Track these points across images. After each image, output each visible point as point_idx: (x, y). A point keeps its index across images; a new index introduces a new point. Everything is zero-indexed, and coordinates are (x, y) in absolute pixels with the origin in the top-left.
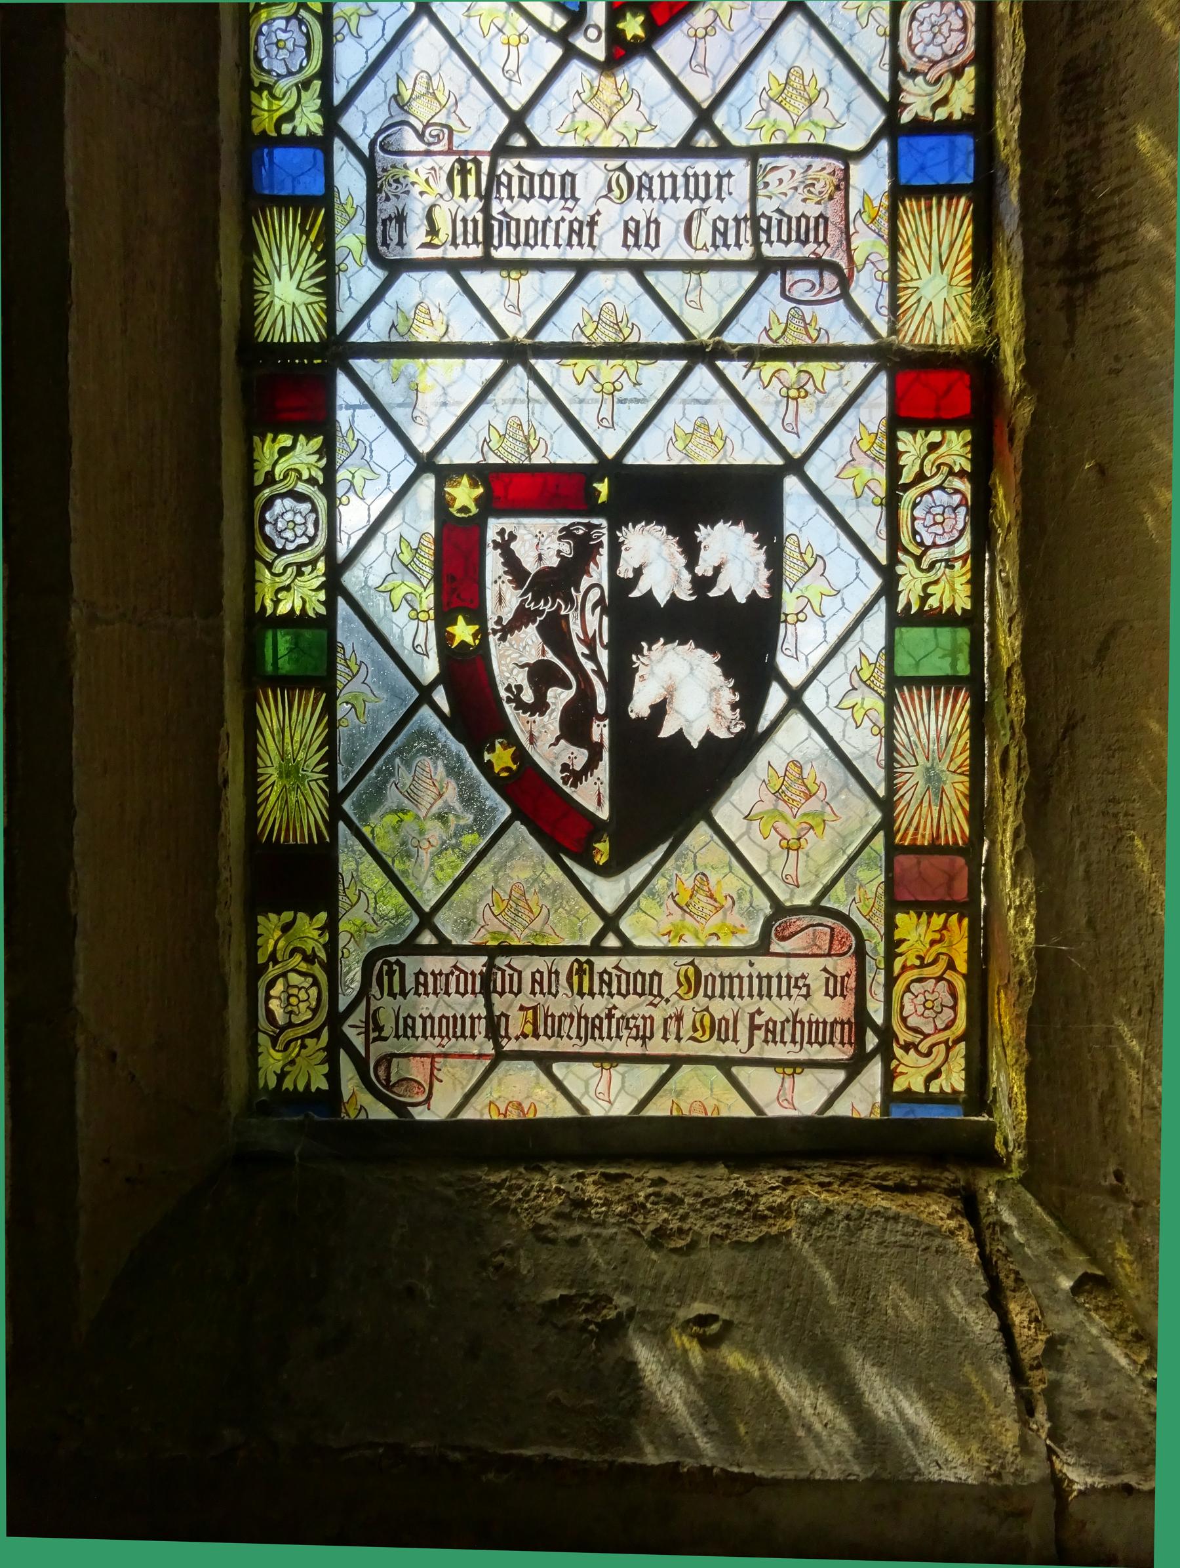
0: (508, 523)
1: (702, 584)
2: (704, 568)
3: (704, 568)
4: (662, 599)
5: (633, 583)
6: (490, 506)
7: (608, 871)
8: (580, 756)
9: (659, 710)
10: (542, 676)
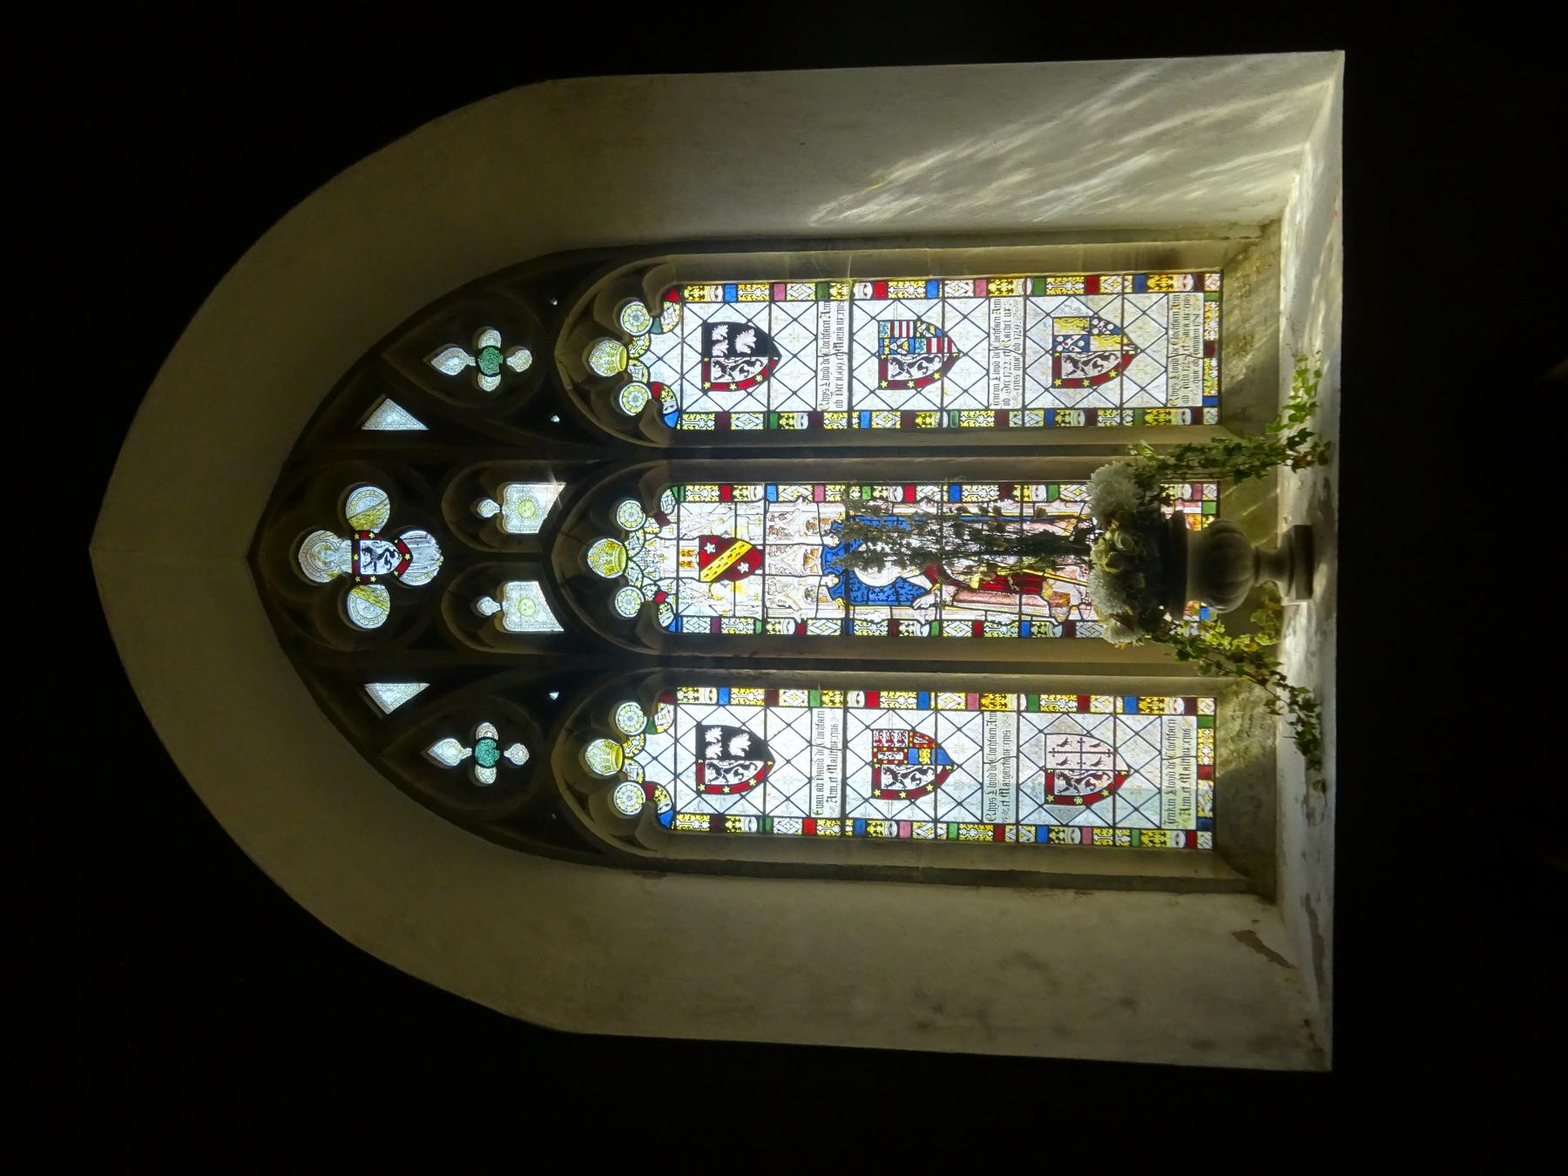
0: (706, 780)
1: (718, 741)
2: (715, 741)
3: (715, 741)
4: (721, 749)
5: (718, 755)
6: (704, 784)
7: (774, 762)
8: (752, 767)
9: (743, 750)
10: (736, 774)
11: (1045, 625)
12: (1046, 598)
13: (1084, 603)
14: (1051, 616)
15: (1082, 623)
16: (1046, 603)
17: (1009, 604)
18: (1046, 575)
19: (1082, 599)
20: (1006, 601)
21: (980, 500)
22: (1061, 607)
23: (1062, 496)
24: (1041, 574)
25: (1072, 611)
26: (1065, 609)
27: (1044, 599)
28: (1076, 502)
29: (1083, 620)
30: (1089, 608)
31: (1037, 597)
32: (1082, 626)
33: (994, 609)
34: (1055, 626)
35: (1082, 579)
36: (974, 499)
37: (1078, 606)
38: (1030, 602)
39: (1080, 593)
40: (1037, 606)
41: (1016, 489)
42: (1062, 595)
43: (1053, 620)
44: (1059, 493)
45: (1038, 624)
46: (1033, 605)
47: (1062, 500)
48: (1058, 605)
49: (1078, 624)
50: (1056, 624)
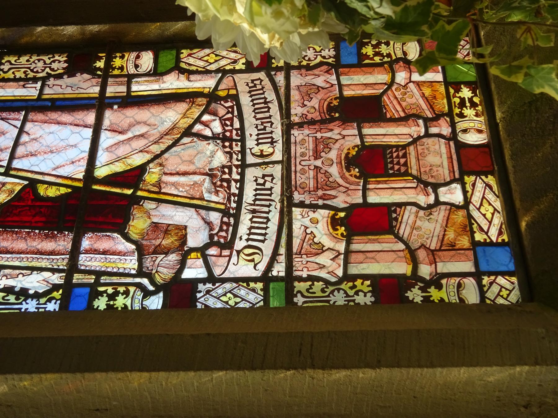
11: (127, 293)
12: (135, 237)
13: (218, 244)
14: (140, 273)
15: (209, 286)
16: (134, 247)
17: (52, 253)
18: (140, 193)
19: (211, 236)
20: (49, 245)
21: (31, 75)
22: (167, 254)
23: (183, 65)
24: (129, 192)
25: (189, 262)
26: (173, 258)
27: (128, 239)
28: (207, 72)
29: (211, 279)
30: (226, 252)
31: (115, 235)
32: (208, 292)
33: (17, 263)
34: (147, 294)
35: (214, 198)
36: (18, 75)
37: (202, 250)
38: (104, 245)
39: (209, 224)
40: (114, 253)
41: (100, 59)
42: (166, 230)
43: (145, 281)
44: (178, 60)
45: (110, 290)
46: (105, 253)
47: (182, 71)
48: (159, 250)
49: (201, 286)
50: (151, 288)
